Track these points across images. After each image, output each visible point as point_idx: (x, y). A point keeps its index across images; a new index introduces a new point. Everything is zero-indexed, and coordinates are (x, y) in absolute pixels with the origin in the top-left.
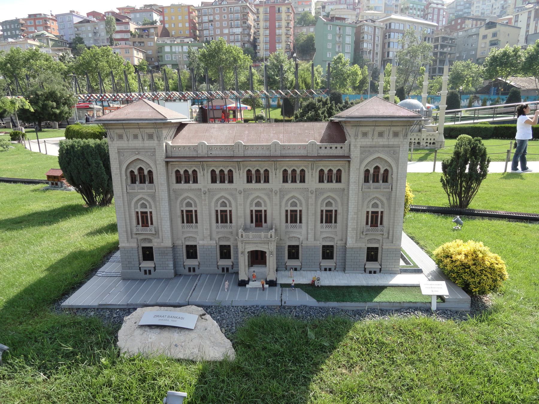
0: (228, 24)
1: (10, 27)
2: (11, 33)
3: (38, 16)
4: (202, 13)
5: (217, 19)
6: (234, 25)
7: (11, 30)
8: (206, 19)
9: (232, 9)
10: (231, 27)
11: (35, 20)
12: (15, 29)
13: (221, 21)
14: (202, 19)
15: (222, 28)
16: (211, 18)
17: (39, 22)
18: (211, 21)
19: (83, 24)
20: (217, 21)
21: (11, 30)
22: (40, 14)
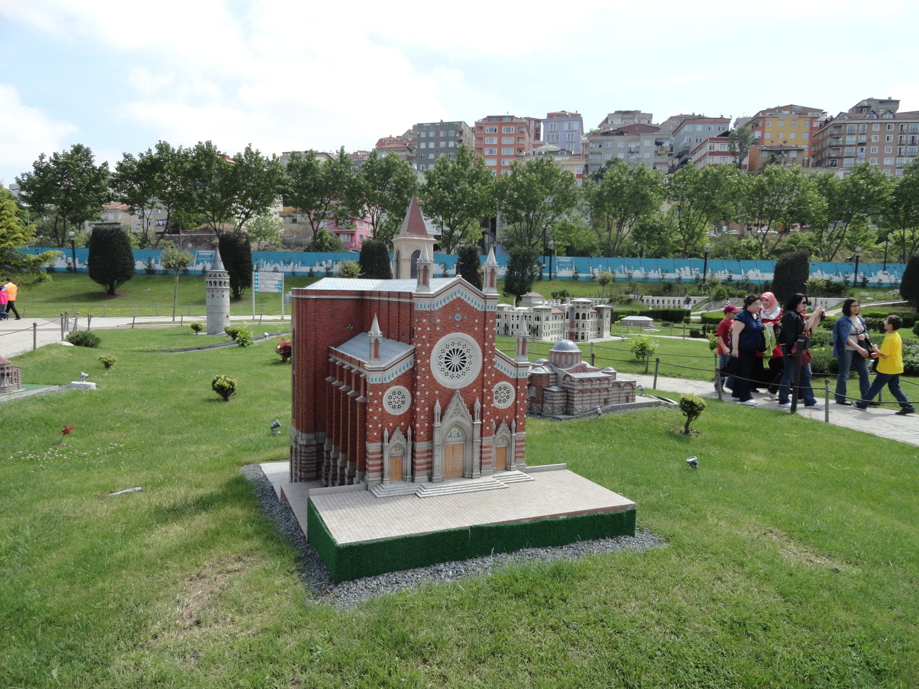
0: (894, 150)
1: (437, 134)
2: (437, 145)
3: (507, 120)
4: (845, 130)
5: (873, 140)
6: (906, 152)
7: (437, 140)
8: (851, 140)
9: (905, 127)
10: (900, 156)
11: (501, 124)
12: (447, 139)
13: (881, 145)
14: (844, 141)
15: (881, 156)
16: (863, 139)
17: (508, 130)
18: (860, 144)
19: (610, 138)
20: (875, 144)
21: (437, 140)
22: (512, 117)
